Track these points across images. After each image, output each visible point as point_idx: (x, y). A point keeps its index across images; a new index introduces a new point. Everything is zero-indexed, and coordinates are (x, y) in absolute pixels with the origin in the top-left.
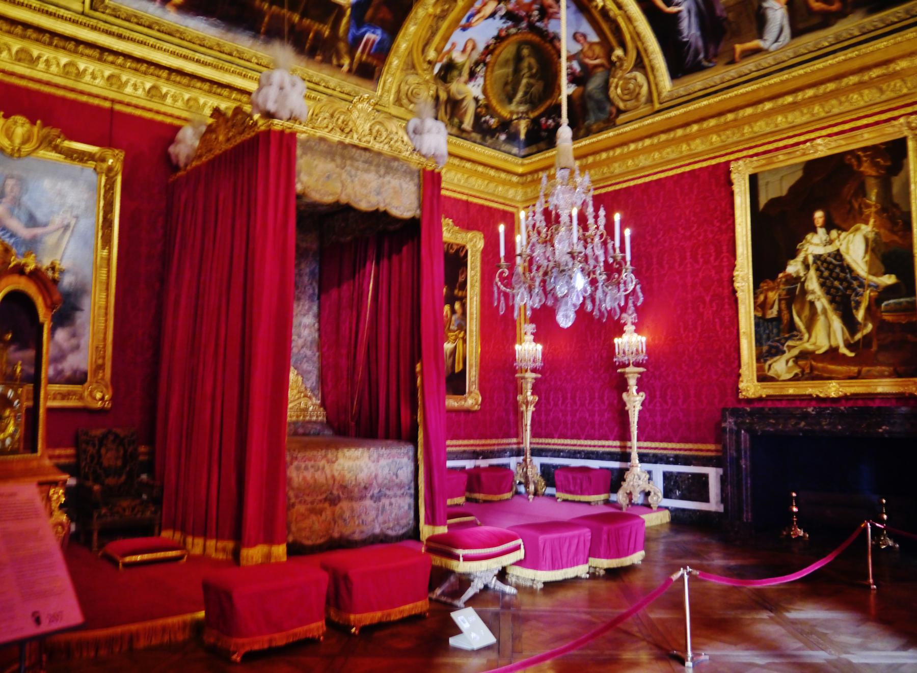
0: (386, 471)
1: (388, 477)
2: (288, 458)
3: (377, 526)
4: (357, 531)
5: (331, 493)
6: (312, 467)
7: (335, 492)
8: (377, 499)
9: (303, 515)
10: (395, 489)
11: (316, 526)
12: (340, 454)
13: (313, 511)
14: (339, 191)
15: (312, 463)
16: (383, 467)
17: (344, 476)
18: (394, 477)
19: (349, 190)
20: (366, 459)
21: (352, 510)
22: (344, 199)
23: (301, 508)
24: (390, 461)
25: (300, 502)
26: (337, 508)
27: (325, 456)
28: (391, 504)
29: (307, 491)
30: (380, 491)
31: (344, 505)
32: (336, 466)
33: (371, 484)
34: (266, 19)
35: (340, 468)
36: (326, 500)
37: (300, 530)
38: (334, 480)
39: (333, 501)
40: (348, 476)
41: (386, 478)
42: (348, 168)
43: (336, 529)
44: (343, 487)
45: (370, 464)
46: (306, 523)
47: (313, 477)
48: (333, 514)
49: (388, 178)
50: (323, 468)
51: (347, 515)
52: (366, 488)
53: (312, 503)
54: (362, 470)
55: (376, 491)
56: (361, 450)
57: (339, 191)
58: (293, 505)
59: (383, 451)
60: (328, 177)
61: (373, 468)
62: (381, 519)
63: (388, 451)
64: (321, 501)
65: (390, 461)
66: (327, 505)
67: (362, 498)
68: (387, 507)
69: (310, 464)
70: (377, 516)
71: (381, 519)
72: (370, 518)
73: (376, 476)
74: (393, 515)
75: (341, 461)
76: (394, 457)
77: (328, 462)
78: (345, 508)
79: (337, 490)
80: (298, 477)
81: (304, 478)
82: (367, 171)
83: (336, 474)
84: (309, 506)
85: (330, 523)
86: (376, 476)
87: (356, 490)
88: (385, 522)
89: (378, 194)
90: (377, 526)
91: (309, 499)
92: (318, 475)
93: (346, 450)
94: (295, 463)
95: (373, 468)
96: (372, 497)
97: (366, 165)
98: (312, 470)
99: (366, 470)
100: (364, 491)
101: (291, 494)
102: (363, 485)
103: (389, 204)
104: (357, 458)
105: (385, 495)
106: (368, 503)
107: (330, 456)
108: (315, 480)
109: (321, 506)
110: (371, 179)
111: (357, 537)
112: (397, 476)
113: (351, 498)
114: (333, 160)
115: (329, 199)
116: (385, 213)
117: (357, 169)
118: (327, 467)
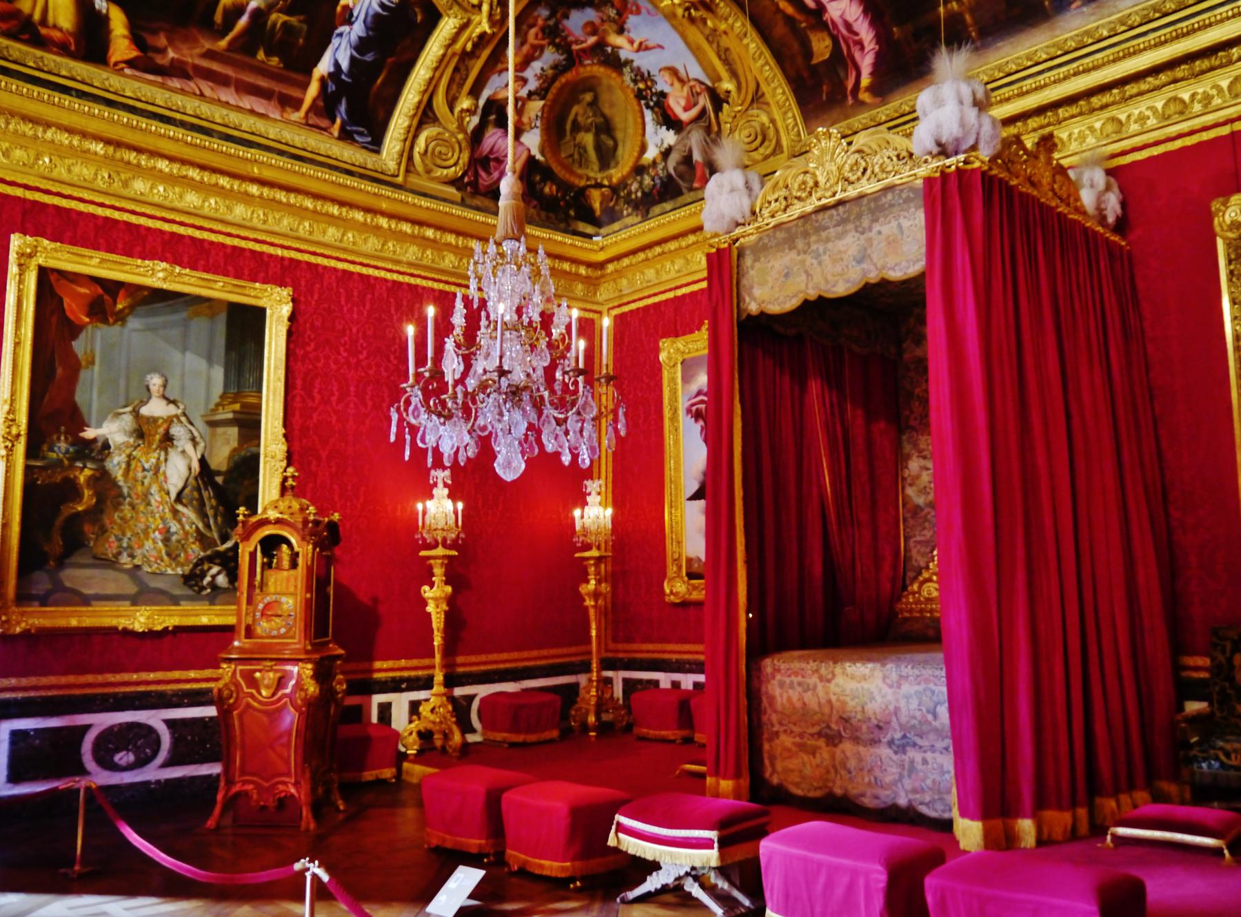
0: (914, 704)
1: (918, 714)
2: (769, 670)
3: (903, 794)
4: (869, 793)
5: (828, 727)
6: (800, 684)
7: (833, 726)
8: (901, 747)
9: (789, 750)
10: (932, 736)
11: (808, 771)
12: (838, 670)
13: (802, 747)
14: (803, 286)
15: (800, 679)
16: (908, 697)
17: (844, 703)
18: (930, 717)
19: (817, 278)
20: (879, 682)
21: (860, 760)
22: (812, 294)
23: (786, 740)
24: (920, 688)
25: (785, 731)
26: (838, 751)
27: (817, 671)
28: (925, 762)
29: (794, 718)
30: (904, 736)
31: (847, 747)
32: (832, 686)
33: (888, 723)
34: (968, 18)
35: (838, 690)
36: (820, 735)
37: (787, 771)
38: (832, 708)
39: (833, 739)
40: (852, 704)
41: (914, 717)
42: (814, 247)
43: (839, 783)
44: (845, 720)
45: (886, 689)
46: (794, 763)
47: (801, 699)
48: (833, 757)
49: (876, 227)
50: (815, 687)
51: (852, 764)
52: (879, 727)
53: (801, 735)
54: (872, 699)
55: (898, 735)
56: (870, 665)
57: (803, 286)
58: (777, 734)
59: (907, 670)
60: (787, 275)
61: (890, 697)
62: (908, 783)
63: (916, 672)
64: (812, 735)
65: (920, 688)
66: (822, 743)
67: (875, 742)
68: (919, 767)
69: (796, 680)
70: (901, 777)
71: (908, 783)
72: (888, 779)
73: (897, 711)
74: (929, 782)
75: (840, 680)
76: (927, 681)
77: (821, 679)
78: (848, 754)
79: (837, 723)
80: (781, 696)
81: (789, 699)
82: (840, 237)
83: (834, 698)
84: (798, 740)
85: (828, 772)
86: (897, 711)
87: (864, 728)
88: (915, 791)
89: (860, 262)
90: (903, 794)
91: (797, 729)
92: (808, 697)
93: (848, 664)
94: (778, 677)
95: (890, 697)
96: (891, 743)
97: (840, 229)
98: (799, 689)
99: (879, 699)
100: (876, 731)
101: (774, 718)
102: (875, 722)
103: (884, 267)
104: (864, 678)
105: (915, 745)
106: (885, 751)
107: (823, 671)
108: (805, 704)
109: (811, 742)
110: (850, 243)
111: (868, 802)
112: (935, 716)
113: (856, 740)
114: (792, 247)
115: (791, 304)
116: (884, 283)
117: (828, 240)
118: (820, 686)
